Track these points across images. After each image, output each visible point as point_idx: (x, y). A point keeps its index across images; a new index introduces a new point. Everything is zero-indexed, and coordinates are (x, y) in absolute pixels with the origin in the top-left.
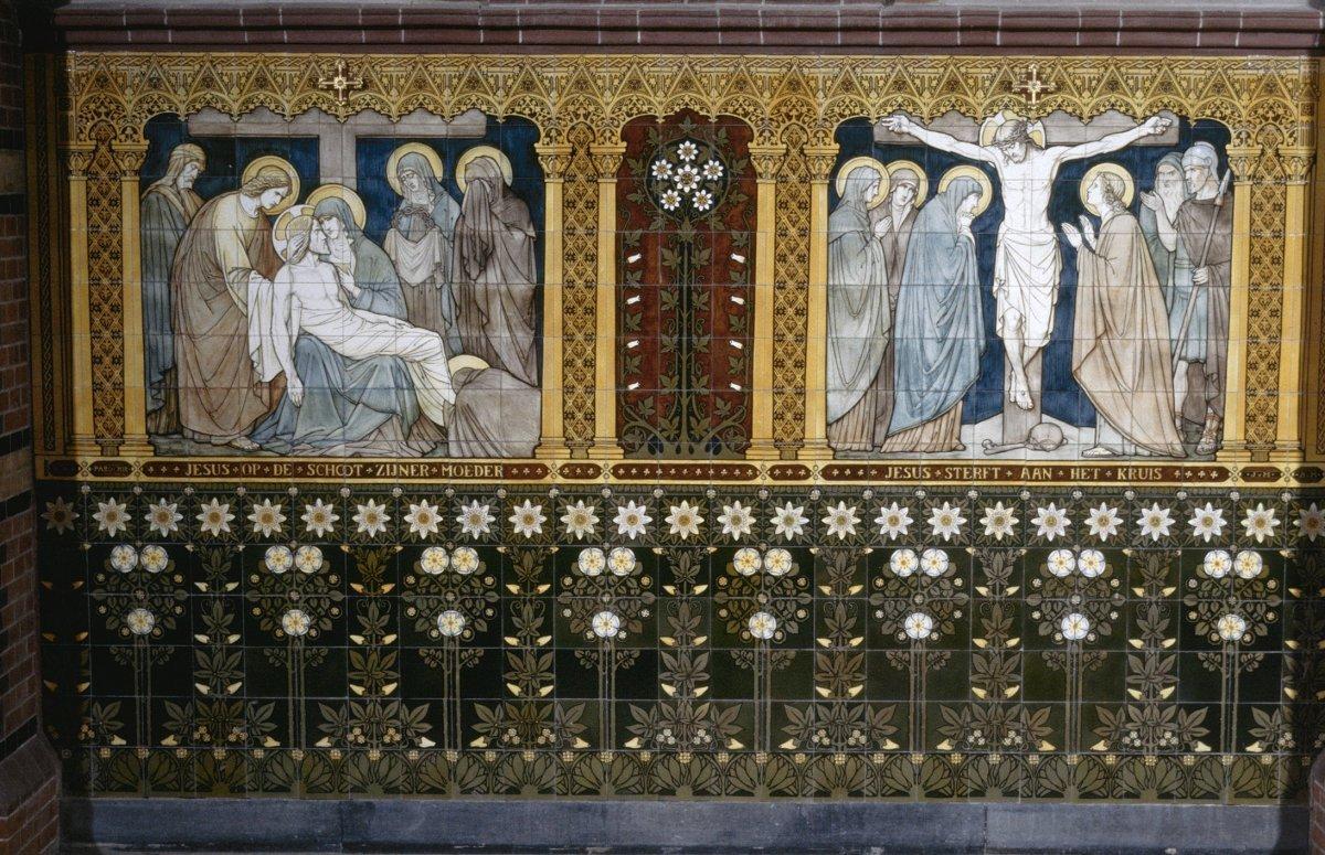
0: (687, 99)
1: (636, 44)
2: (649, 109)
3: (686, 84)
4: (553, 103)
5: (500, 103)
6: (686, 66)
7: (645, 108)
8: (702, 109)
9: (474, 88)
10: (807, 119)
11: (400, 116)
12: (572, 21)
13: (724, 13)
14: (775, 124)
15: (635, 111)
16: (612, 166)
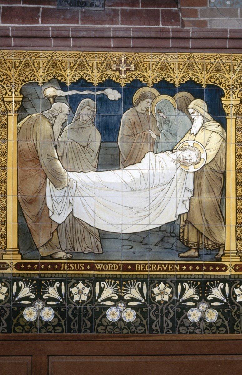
0: (191, 75)
1: (129, 47)
2: (34, 79)
3: (81, 66)
4: (41, 75)
5: (96, 76)
6: (109, 57)
7: (32, 78)
8: (89, 79)
9: (54, 68)
10: (6, 82)
11: (43, 83)
12: (93, 34)
13: (135, 30)
14: (17, 85)
15: (27, 79)
16: (13, 108)
